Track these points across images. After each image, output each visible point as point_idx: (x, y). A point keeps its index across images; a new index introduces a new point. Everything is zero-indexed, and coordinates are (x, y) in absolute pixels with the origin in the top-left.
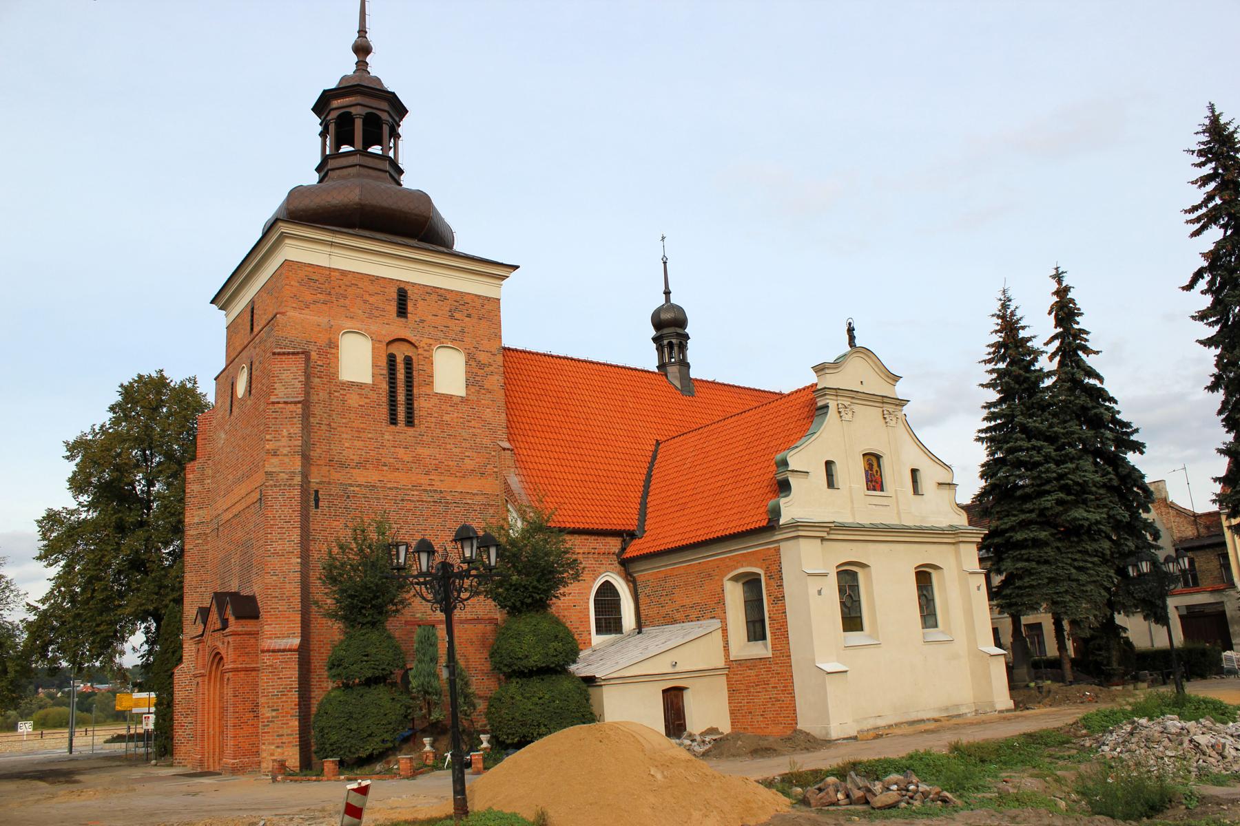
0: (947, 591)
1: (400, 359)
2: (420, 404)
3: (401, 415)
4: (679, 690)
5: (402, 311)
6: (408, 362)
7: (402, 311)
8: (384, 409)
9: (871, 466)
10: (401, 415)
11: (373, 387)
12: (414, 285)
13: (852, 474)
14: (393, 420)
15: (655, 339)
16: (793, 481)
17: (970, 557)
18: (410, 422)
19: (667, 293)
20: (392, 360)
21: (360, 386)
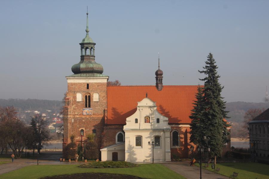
0: (162, 140)
1: (88, 96)
2: (91, 103)
3: (88, 106)
4: (117, 153)
5: (88, 88)
6: (89, 96)
7: (88, 88)
8: (85, 104)
9: (147, 119)
10: (88, 106)
11: (83, 101)
12: (90, 83)
13: (142, 120)
14: (86, 107)
15: (156, 77)
16: (127, 122)
17: (168, 134)
18: (89, 107)
19: (159, 67)
20: (86, 96)
21: (80, 102)
